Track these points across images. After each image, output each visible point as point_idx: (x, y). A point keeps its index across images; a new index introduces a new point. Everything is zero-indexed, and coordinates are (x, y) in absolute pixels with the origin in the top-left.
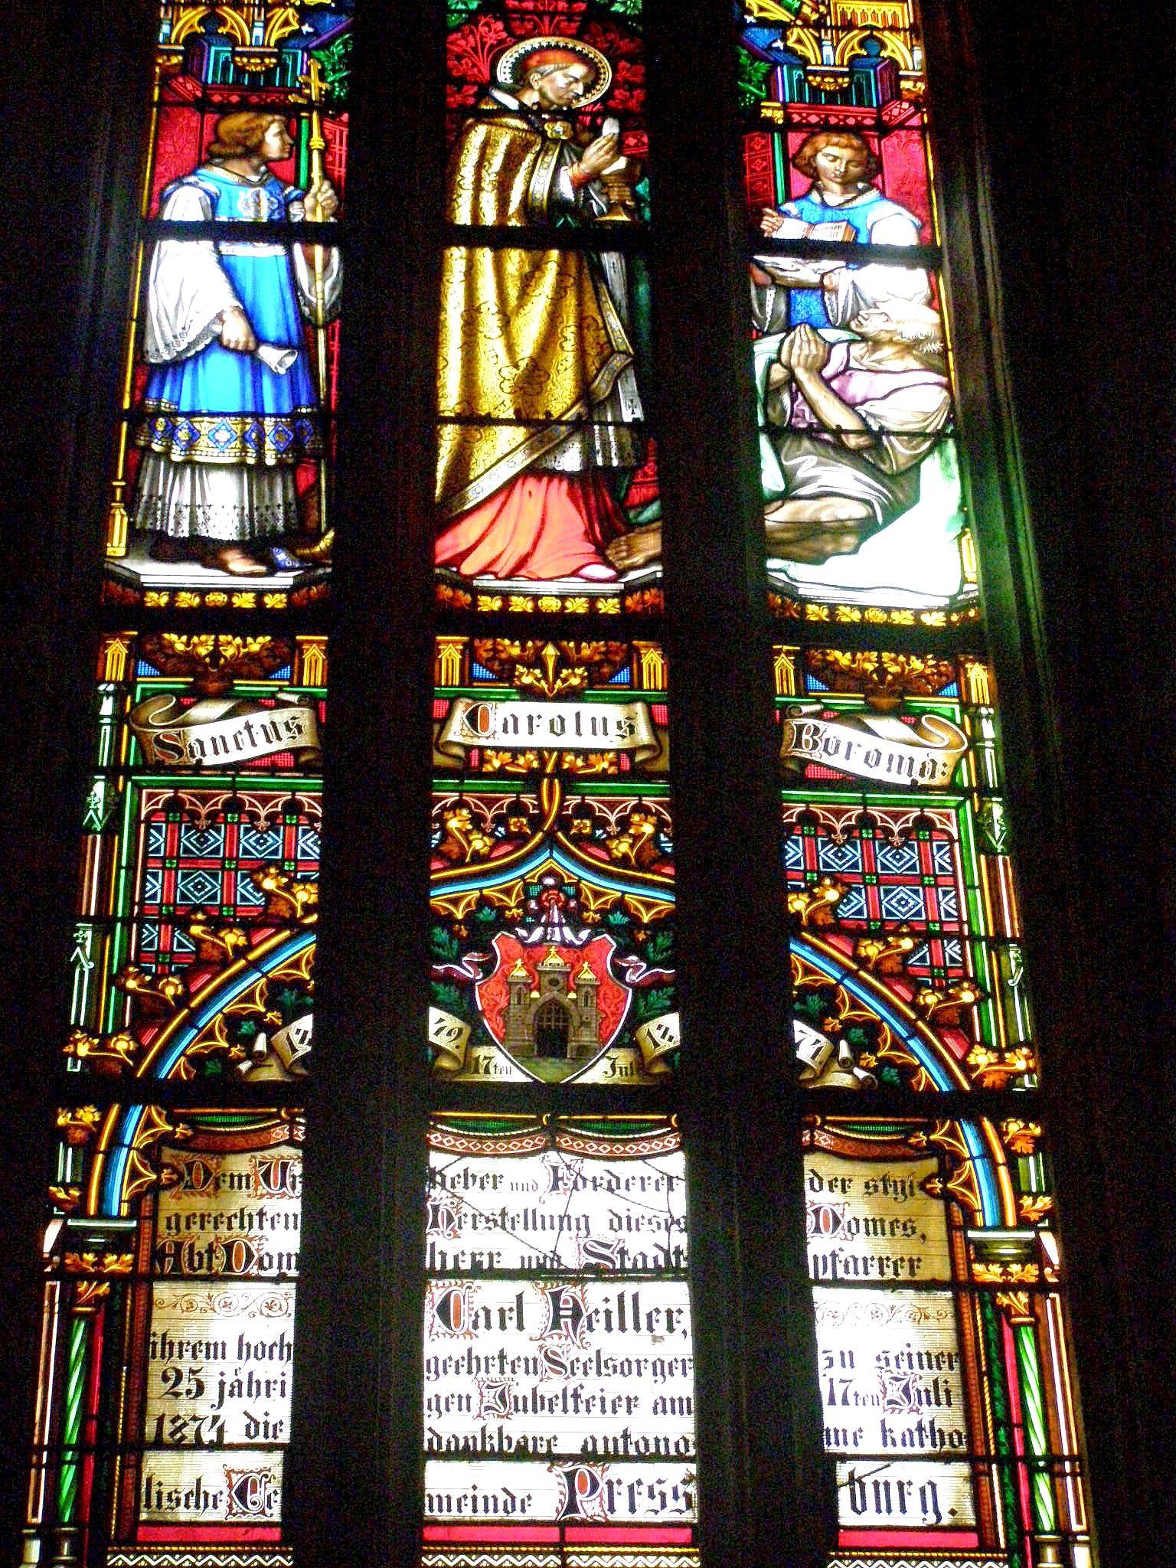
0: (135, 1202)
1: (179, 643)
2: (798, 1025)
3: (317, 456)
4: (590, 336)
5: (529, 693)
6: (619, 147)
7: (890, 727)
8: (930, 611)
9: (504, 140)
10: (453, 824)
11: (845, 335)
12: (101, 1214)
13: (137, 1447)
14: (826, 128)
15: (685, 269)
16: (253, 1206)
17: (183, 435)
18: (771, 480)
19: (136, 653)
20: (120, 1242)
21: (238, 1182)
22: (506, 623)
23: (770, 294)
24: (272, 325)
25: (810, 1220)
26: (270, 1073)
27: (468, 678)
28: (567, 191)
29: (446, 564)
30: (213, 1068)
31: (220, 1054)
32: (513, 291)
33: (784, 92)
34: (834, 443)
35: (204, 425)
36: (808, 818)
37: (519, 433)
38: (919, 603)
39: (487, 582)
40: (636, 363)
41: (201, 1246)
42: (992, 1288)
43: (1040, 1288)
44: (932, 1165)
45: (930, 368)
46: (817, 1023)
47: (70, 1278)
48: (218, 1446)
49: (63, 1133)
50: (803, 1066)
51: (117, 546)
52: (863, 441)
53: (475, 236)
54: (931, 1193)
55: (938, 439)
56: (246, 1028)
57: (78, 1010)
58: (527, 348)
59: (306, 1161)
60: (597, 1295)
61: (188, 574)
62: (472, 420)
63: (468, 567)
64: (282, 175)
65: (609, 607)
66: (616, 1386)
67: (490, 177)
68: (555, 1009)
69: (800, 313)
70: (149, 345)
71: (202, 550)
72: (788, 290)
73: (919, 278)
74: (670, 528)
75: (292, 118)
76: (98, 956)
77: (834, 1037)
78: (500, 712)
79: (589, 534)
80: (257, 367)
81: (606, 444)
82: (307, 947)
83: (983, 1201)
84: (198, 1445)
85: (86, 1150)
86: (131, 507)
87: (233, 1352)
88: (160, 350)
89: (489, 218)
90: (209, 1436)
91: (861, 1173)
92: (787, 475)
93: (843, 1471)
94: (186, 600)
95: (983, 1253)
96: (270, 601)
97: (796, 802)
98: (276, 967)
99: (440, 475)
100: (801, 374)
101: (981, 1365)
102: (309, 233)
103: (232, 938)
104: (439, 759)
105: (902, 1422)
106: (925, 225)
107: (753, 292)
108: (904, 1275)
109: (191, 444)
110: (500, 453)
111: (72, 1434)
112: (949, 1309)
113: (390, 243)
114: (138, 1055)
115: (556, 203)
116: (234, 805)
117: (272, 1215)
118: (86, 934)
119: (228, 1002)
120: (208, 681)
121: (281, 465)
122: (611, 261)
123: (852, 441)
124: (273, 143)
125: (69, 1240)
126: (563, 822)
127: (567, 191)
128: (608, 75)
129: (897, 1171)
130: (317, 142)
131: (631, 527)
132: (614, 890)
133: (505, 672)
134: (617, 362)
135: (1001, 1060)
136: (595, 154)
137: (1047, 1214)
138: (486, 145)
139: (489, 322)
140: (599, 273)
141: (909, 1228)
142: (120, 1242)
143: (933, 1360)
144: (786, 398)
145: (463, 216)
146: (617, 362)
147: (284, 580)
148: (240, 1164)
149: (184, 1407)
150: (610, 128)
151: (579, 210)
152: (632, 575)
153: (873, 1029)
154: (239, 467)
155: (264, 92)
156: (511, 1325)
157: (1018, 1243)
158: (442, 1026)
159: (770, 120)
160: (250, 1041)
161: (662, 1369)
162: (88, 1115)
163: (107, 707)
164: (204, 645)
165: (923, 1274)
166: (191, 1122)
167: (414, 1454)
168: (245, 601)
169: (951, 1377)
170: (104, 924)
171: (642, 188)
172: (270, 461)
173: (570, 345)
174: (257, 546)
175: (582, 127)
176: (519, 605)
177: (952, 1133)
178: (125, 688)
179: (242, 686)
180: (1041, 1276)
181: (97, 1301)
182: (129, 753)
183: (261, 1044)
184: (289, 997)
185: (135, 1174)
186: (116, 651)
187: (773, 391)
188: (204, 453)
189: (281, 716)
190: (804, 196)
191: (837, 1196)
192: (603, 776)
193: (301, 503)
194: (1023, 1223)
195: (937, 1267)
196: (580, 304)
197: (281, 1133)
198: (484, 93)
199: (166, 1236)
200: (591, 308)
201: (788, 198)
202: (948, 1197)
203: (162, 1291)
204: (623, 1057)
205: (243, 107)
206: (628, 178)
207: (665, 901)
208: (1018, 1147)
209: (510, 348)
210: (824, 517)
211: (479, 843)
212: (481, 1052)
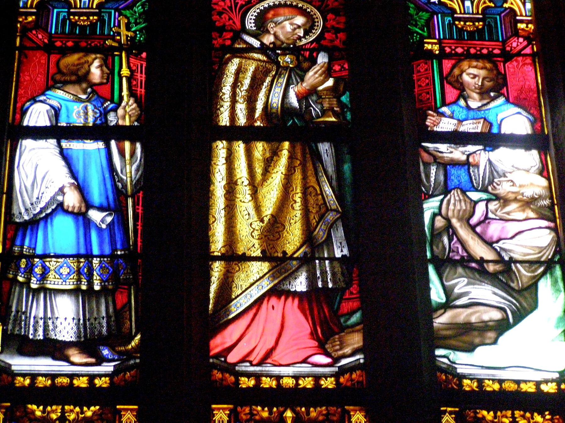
3: (127, 283)
4: (312, 200)
6: (328, 72)
8: (546, 382)
9: (251, 68)
11: (484, 196)
14: (467, 56)
17: (38, 270)
18: (437, 295)
22: (259, 395)
23: (433, 169)
24: (97, 195)
28: (293, 101)
29: (217, 356)
32: (259, 170)
33: (440, 33)
34: (478, 270)
35: (52, 264)
37: (265, 266)
38: (539, 377)
39: (246, 367)
40: (344, 217)
45: (542, 217)
52: (498, 267)
53: (232, 133)
55: (549, 265)
58: (268, 209)
61: (43, 364)
62: (234, 258)
63: (232, 358)
64: (102, 94)
65: (328, 383)
69: (453, 181)
70: (15, 211)
71: (54, 349)
72: (446, 166)
73: (532, 158)
74: (369, 329)
75: (108, 57)
79: (313, 335)
80: (87, 224)
81: (324, 272)
92: (448, 292)
94: (42, 382)
96: (98, 382)
99: (212, 295)
100: (454, 221)
102: (121, 133)
106: (536, 121)
107: (422, 167)
109: (44, 276)
110: (253, 279)
113: (175, 141)
122: (324, 148)
123: (491, 268)
124: (96, 73)
127: (293, 101)
128: (320, 23)
130: (125, 72)
131: (343, 329)
134: (330, 217)
136: (312, 76)
138: (239, 72)
139: (244, 192)
140: (317, 157)
144: (446, 240)
145: (224, 120)
146: (330, 217)
147: (108, 368)
150: (322, 59)
151: (302, 113)
152: (344, 362)
154: (75, 292)
155: (90, 39)
159: (431, 51)
168: (82, 383)
171: (345, 99)
172: (97, 288)
173: (298, 206)
174: (89, 344)
175: (304, 58)
176: (267, 383)
187: (436, 235)
188: (53, 282)
190: (455, 102)
193: (118, 316)
196: (305, 178)
200: (312, 181)
201: (444, 104)
205: (75, 50)
206: (334, 91)
209: (258, 208)
210: (473, 319)
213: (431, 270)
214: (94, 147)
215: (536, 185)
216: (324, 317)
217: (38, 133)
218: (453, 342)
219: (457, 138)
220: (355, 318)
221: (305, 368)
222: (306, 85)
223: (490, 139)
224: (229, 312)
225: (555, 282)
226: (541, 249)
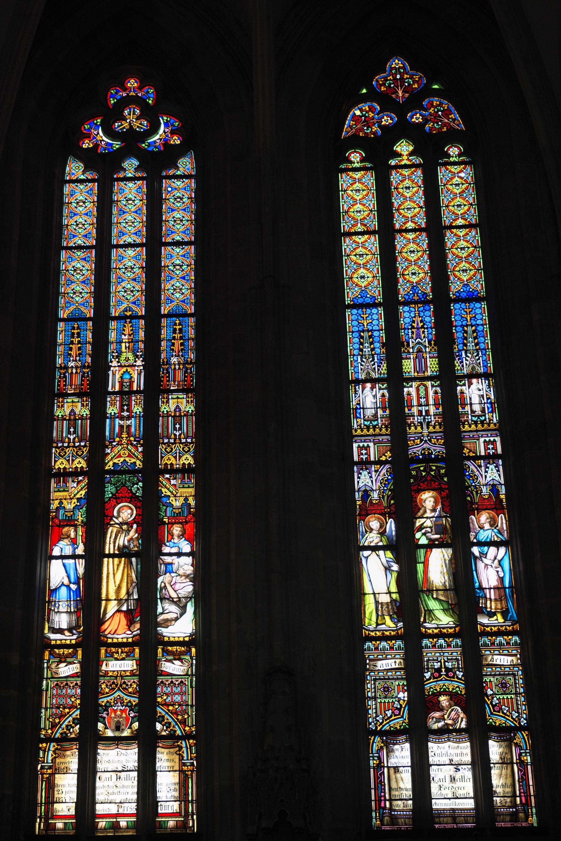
0: (52, 760)
1: (57, 651)
2: (157, 723)
4: (129, 578)
5: (117, 659)
6: (136, 531)
7: (177, 662)
8: (186, 637)
9: (115, 530)
10: (103, 686)
11: (176, 574)
12: (47, 763)
13: (53, 803)
15: (147, 560)
16: (70, 760)
17: (57, 605)
19: (50, 654)
20: (50, 768)
21: (68, 756)
23: (163, 566)
24: (73, 580)
25: (157, 760)
26: (73, 736)
27: (106, 657)
28: (126, 543)
29: (102, 632)
30: (64, 735)
31: (65, 732)
32: (116, 569)
33: (168, 514)
34: (171, 600)
35: (60, 603)
36: (162, 682)
37: (116, 602)
38: (184, 635)
39: (109, 636)
40: (137, 585)
41: (62, 768)
42: (186, 771)
43: (192, 771)
44: (177, 749)
45: (191, 581)
46: (161, 723)
47: (42, 774)
48: (65, 802)
49: (40, 748)
50: (158, 731)
51: (46, 631)
52: (177, 599)
53: (109, 556)
54: (177, 754)
55: (191, 598)
56: (69, 727)
57: (42, 726)
58: (118, 583)
59: (78, 752)
60: (123, 775)
61: (58, 636)
62: (108, 600)
63: (106, 633)
66: (125, 790)
67: (112, 540)
68: (118, 722)
70: (51, 585)
71: (60, 631)
72: (167, 564)
73: (189, 560)
74: (141, 622)
76: (45, 715)
77: (163, 725)
78: (111, 663)
79: (127, 625)
81: (131, 604)
82: (78, 712)
83: (185, 755)
84: (62, 802)
85: (44, 751)
86: (48, 623)
87: (67, 786)
88: (53, 587)
89: (112, 552)
90: (64, 801)
91: (166, 751)
92: (163, 608)
93: (159, 804)
94: (59, 642)
95: (184, 765)
97: (160, 679)
98: (74, 716)
99: (102, 612)
100: (167, 585)
101: (183, 785)
103: (67, 710)
104: (101, 674)
105: (169, 795)
106: (192, 547)
107: (159, 566)
108: (171, 769)
110: (112, 607)
111: (43, 802)
112: (178, 775)
113: (94, 557)
114: (52, 733)
115: (124, 546)
116: (67, 684)
117: (72, 761)
118: (43, 711)
119: (66, 723)
120: (62, 659)
121: (74, 611)
122: (134, 560)
123: (175, 600)
124: (72, 535)
125: (42, 768)
126: (121, 685)
127: (126, 543)
128: (135, 512)
129: (172, 750)
131: (135, 622)
132: (129, 698)
133: (112, 656)
135: (190, 729)
136: (132, 533)
137: (195, 757)
138: (112, 532)
139: (111, 576)
140: (131, 563)
141: (173, 761)
142: (50, 768)
143: (175, 784)
144: (164, 590)
145: (107, 552)
146: (134, 584)
147: (75, 637)
148: (68, 753)
149: (60, 796)
150: (135, 526)
152: (134, 633)
153: (170, 723)
154: (67, 612)
155: (70, 522)
156: (110, 780)
157: (190, 763)
158: (100, 726)
159: (165, 521)
160: (69, 730)
161: (132, 787)
162: (44, 745)
163: (45, 665)
164: (61, 651)
165: (175, 769)
166: (61, 746)
167: (94, 803)
168: (68, 642)
169: (177, 787)
170: (46, 709)
171: (140, 541)
172: (72, 611)
173: (125, 581)
174: (70, 630)
175: (130, 525)
176: (115, 641)
177: (181, 743)
178: (49, 660)
179: (68, 660)
180: (193, 769)
181: (47, 778)
182: (50, 676)
183: (71, 731)
184: (76, 721)
185: (52, 755)
186: (47, 653)
188: (61, 609)
189: (74, 665)
190: (170, 541)
191: (162, 755)
192: (128, 676)
194: (191, 759)
195: (177, 768)
196: (128, 571)
197: (75, 747)
198: (111, 519)
199: (57, 766)
200: (129, 571)
201: (168, 542)
202: (179, 755)
203: (57, 776)
204: (129, 731)
205: (67, 525)
206: (137, 539)
207: (137, 700)
208: (192, 745)
209: (115, 582)
210: (169, 617)
211: (107, 690)
212: (107, 730)
213: (159, 600)
214: (72, 561)
215: (189, 570)
216: (130, 616)
217: (57, 558)
218: (163, 625)
219: (170, 554)
220: (138, 619)
221: (125, 636)
222: (129, 537)
223: (179, 554)
224: (106, 618)
225: (192, 604)
226: (189, 592)
